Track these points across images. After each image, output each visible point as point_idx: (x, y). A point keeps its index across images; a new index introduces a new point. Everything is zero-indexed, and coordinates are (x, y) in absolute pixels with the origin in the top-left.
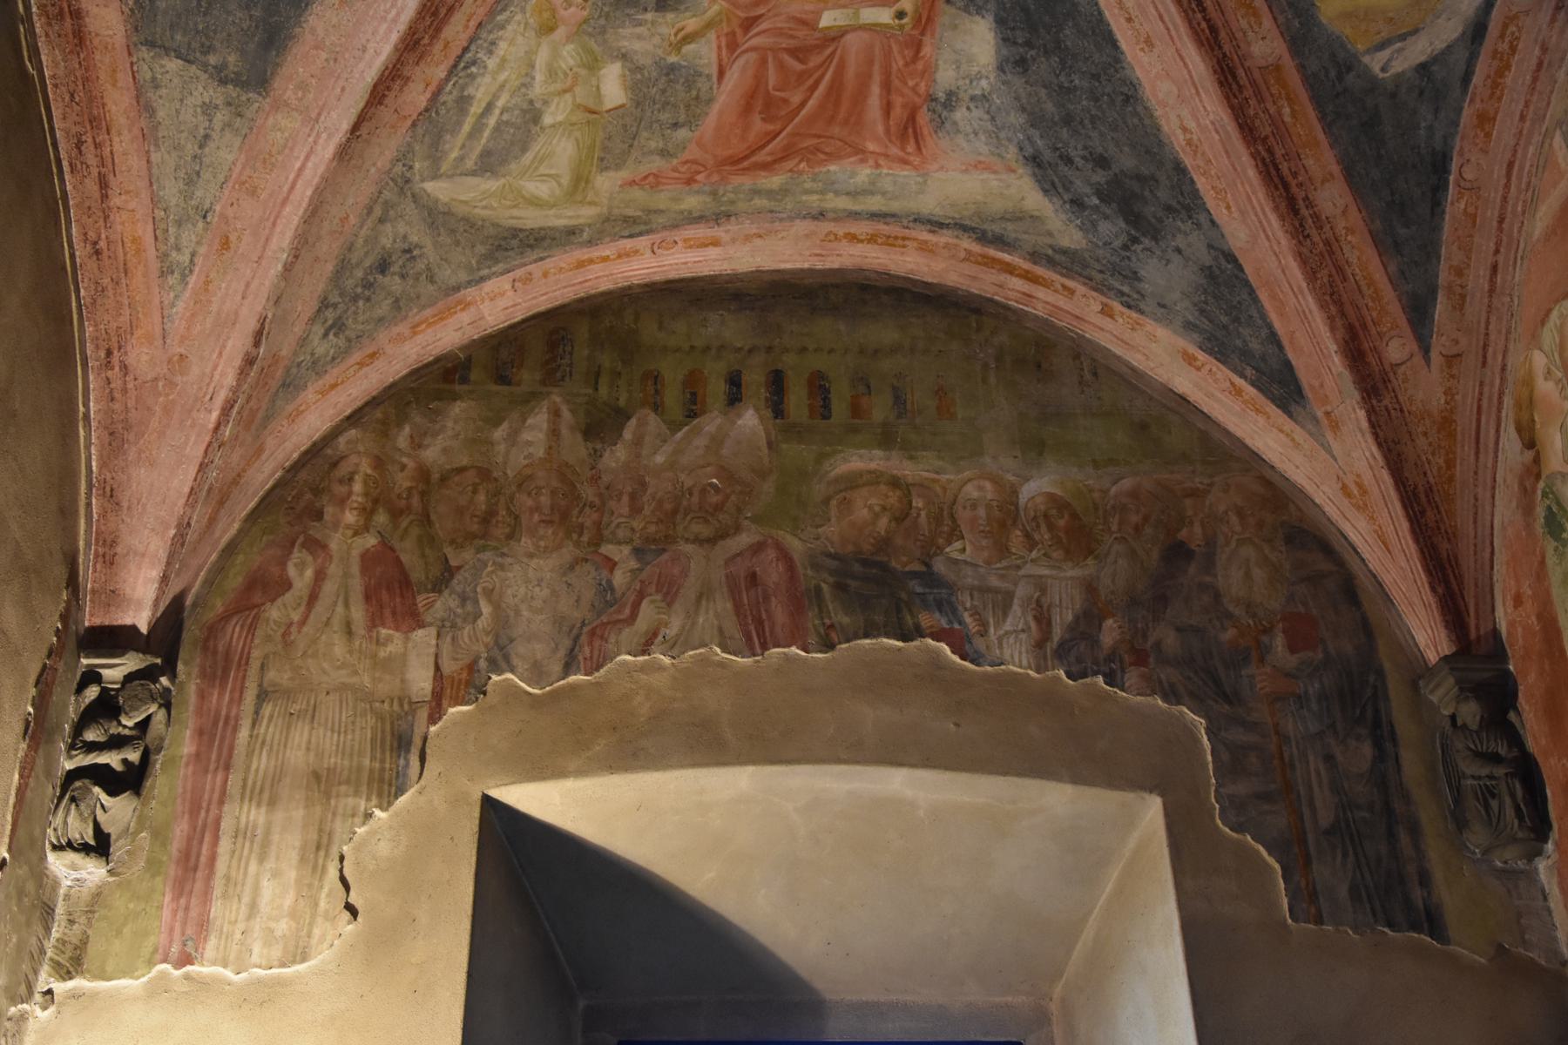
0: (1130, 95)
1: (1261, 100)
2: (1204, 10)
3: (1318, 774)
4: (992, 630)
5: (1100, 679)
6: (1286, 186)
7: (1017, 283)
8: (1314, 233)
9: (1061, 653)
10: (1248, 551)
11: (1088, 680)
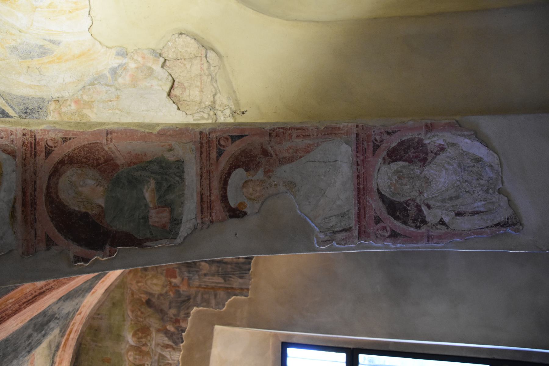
3: (209, 279)
4: (170, 362)
5: (183, 334)
6: (35, 296)
7: (72, 336)
8: (51, 285)
9: (176, 343)
10: (149, 282)
11: (184, 337)
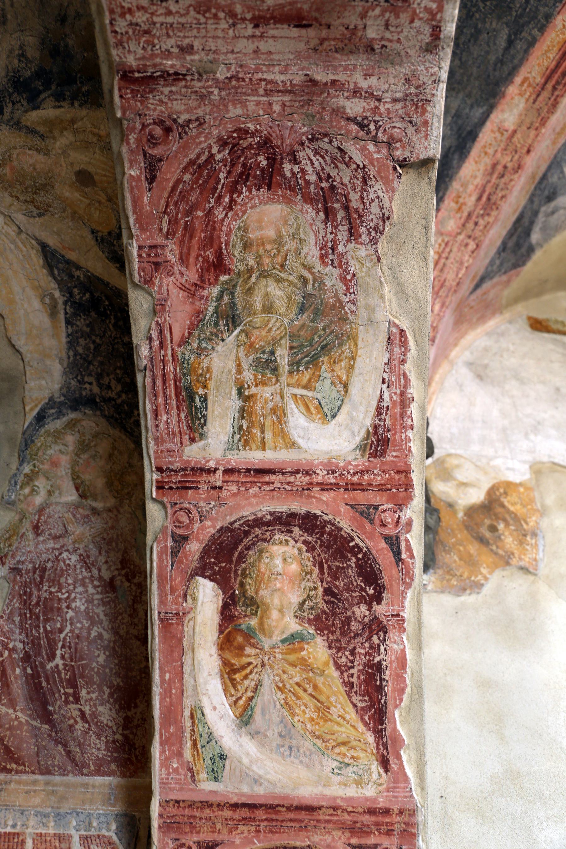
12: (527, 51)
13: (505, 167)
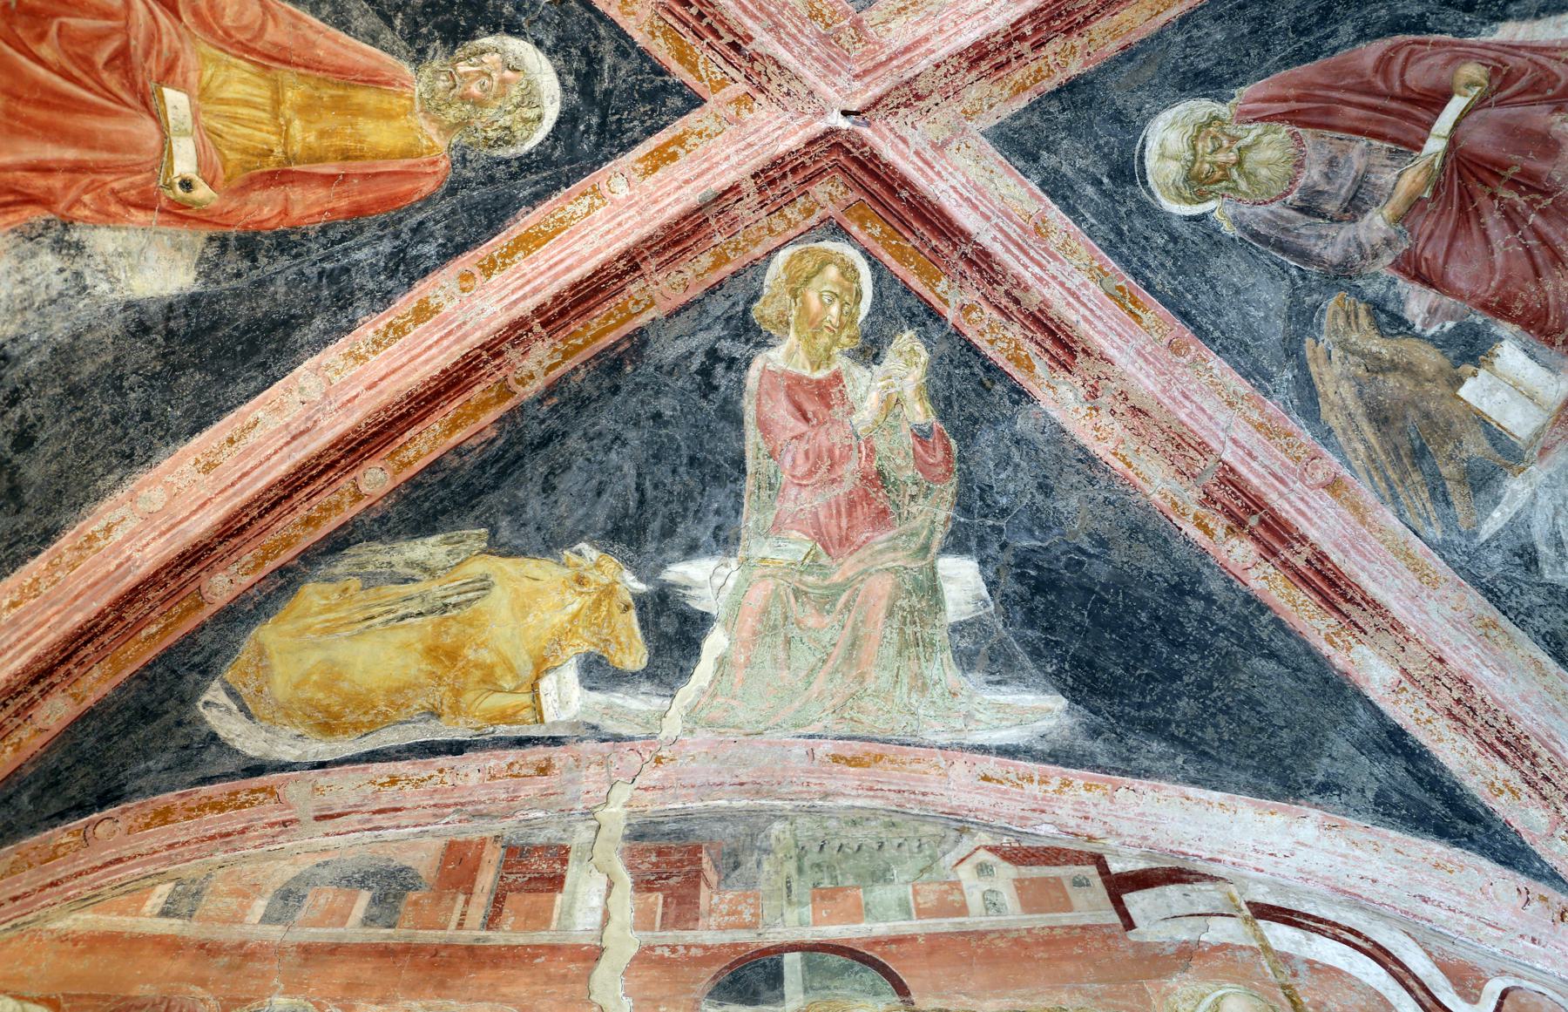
0: (131, 458)
1: (163, 601)
2: (261, 516)
12: (1289, 633)
13: (1459, 701)
